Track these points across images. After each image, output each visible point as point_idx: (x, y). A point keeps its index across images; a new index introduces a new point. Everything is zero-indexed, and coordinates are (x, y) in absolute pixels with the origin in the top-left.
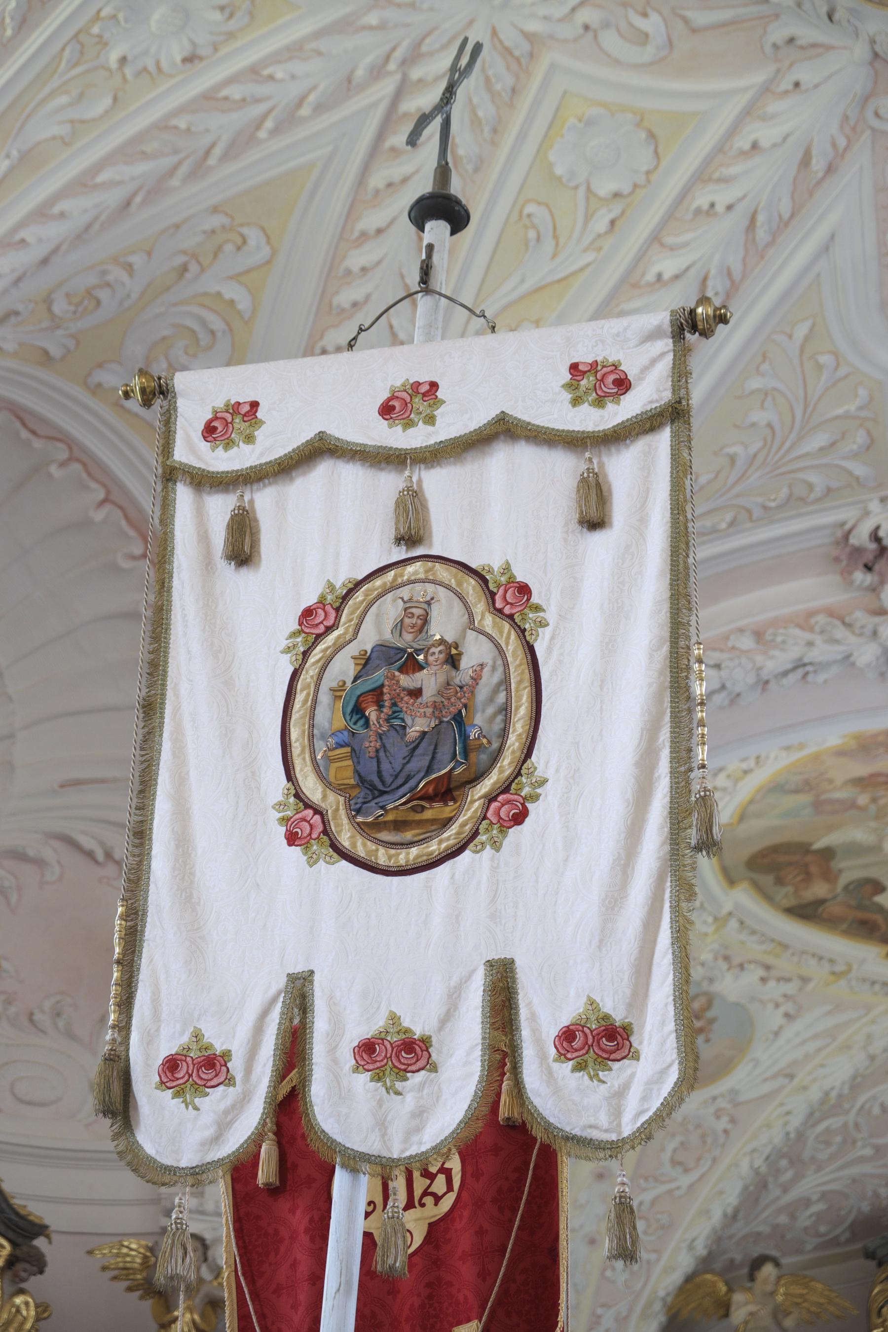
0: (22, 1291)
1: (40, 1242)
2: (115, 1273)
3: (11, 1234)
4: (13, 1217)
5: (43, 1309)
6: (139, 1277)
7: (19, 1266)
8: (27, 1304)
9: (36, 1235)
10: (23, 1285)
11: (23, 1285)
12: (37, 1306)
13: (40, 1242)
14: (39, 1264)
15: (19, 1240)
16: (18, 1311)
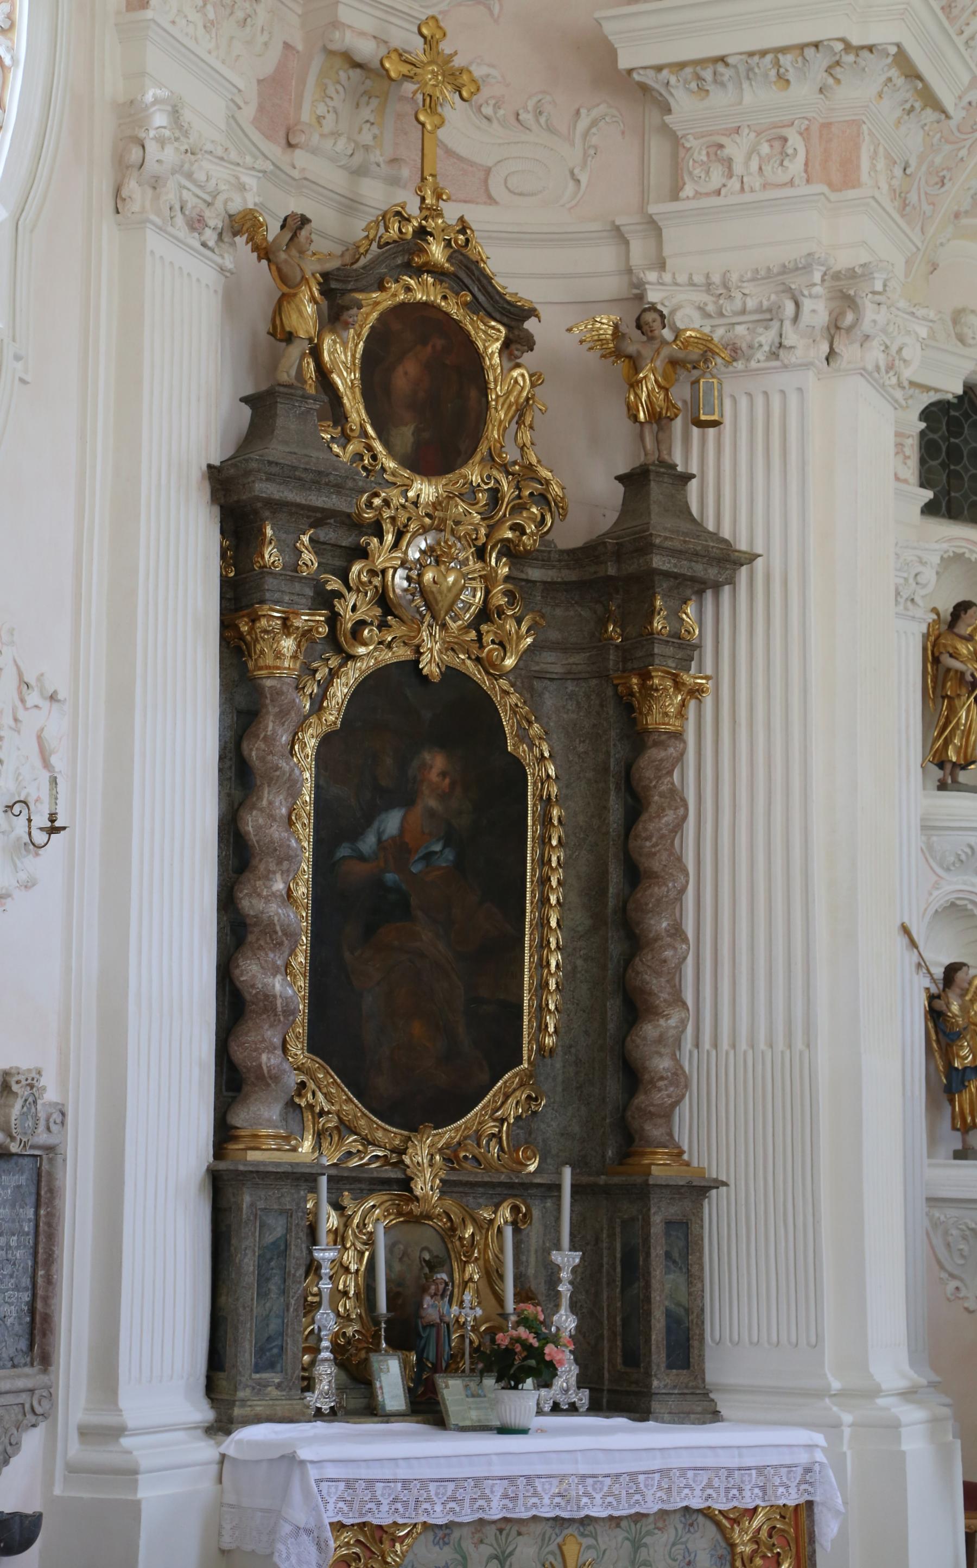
0: (518, 366)
1: (530, 325)
2: (589, 345)
3: (505, 320)
4: (505, 306)
5: (536, 379)
6: (611, 345)
7: (513, 347)
8: (523, 376)
9: (528, 318)
10: (518, 361)
11: (518, 361)
12: (531, 376)
13: (530, 325)
14: (528, 343)
15: (513, 324)
16: (516, 382)
